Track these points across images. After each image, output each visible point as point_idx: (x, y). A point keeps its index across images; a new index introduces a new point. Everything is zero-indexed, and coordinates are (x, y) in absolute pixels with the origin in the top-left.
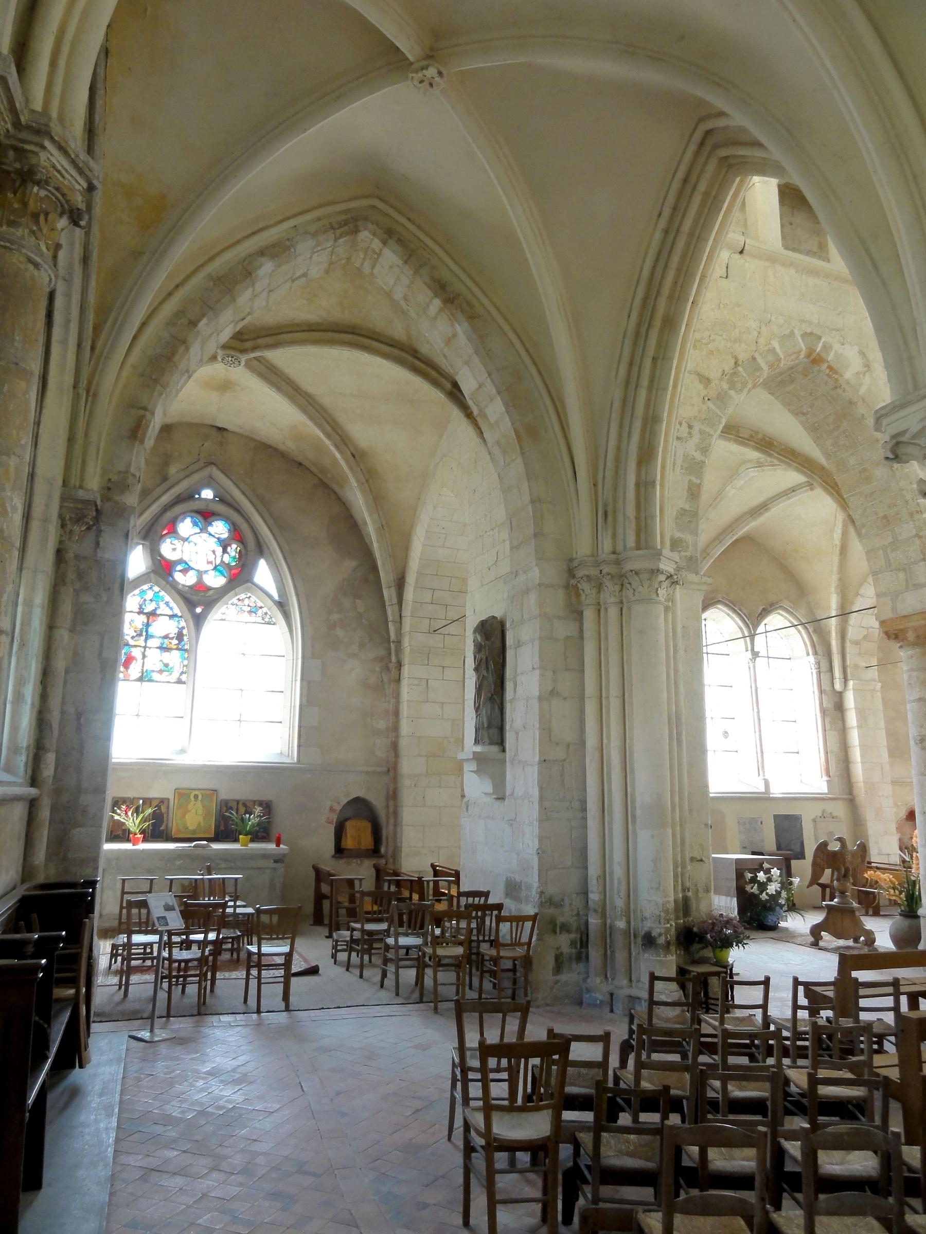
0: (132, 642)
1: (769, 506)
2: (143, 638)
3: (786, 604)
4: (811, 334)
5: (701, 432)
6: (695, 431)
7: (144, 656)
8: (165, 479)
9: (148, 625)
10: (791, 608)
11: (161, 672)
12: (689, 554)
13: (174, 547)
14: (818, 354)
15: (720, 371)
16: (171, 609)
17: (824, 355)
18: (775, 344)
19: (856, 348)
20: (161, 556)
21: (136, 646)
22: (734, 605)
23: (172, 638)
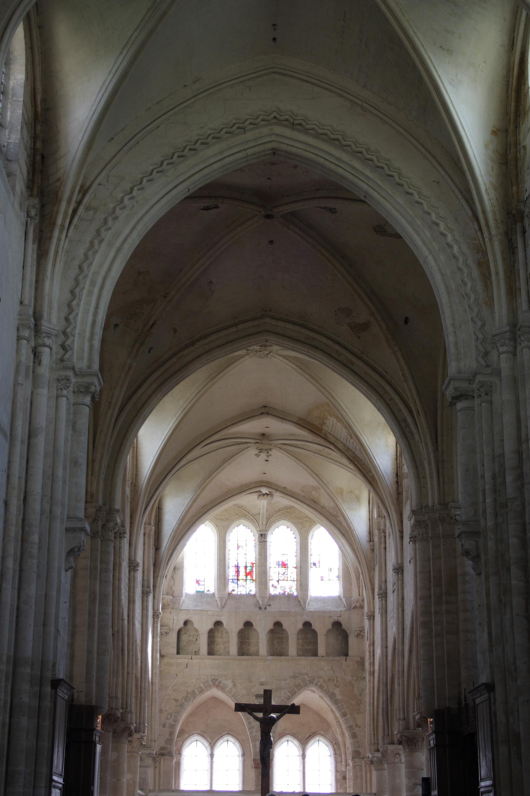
3: (322, 732)
4: (215, 679)
5: (174, 716)
6: (173, 717)
10: (324, 734)
12: (168, 751)
18: (202, 685)
19: (231, 680)
22: (295, 736)
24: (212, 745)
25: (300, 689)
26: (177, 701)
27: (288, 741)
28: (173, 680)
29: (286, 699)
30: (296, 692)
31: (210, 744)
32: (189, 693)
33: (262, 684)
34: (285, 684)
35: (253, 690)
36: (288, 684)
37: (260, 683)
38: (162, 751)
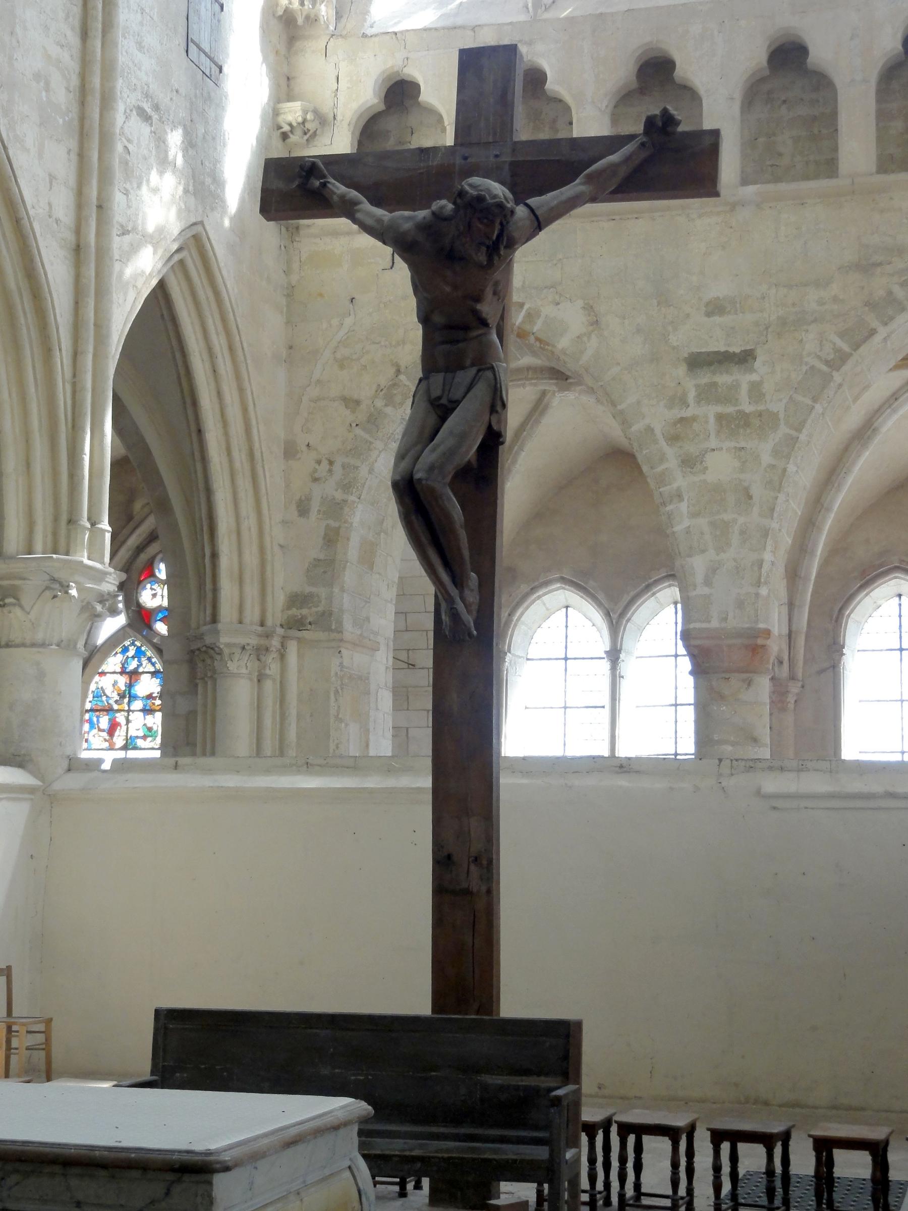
0: (116, 707)
1: (876, 425)
2: (126, 700)
6: (337, 468)
7: (128, 721)
8: (130, 518)
9: (130, 686)
11: (144, 737)
12: (320, 609)
13: (154, 592)
14: (519, 328)
15: (374, 387)
16: (153, 664)
17: (527, 327)
19: (580, 303)
20: (139, 605)
21: (119, 711)
23: (154, 698)
24: (614, 616)
25: (892, 318)
26: (351, 403)
27: (900, 596)
28: (335, 322)
29: (827, 363)
30: (873, 332)
31: (608, 614)
32: (402, 369)
33: (715, 308)
34: (821, 303)
35: (674, 340)
36: (835, 299)
37: (707, 304)
38: (294, 611)
